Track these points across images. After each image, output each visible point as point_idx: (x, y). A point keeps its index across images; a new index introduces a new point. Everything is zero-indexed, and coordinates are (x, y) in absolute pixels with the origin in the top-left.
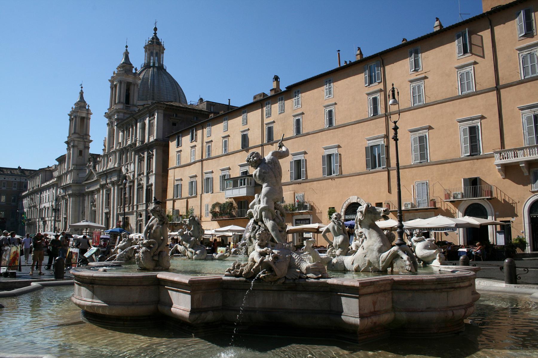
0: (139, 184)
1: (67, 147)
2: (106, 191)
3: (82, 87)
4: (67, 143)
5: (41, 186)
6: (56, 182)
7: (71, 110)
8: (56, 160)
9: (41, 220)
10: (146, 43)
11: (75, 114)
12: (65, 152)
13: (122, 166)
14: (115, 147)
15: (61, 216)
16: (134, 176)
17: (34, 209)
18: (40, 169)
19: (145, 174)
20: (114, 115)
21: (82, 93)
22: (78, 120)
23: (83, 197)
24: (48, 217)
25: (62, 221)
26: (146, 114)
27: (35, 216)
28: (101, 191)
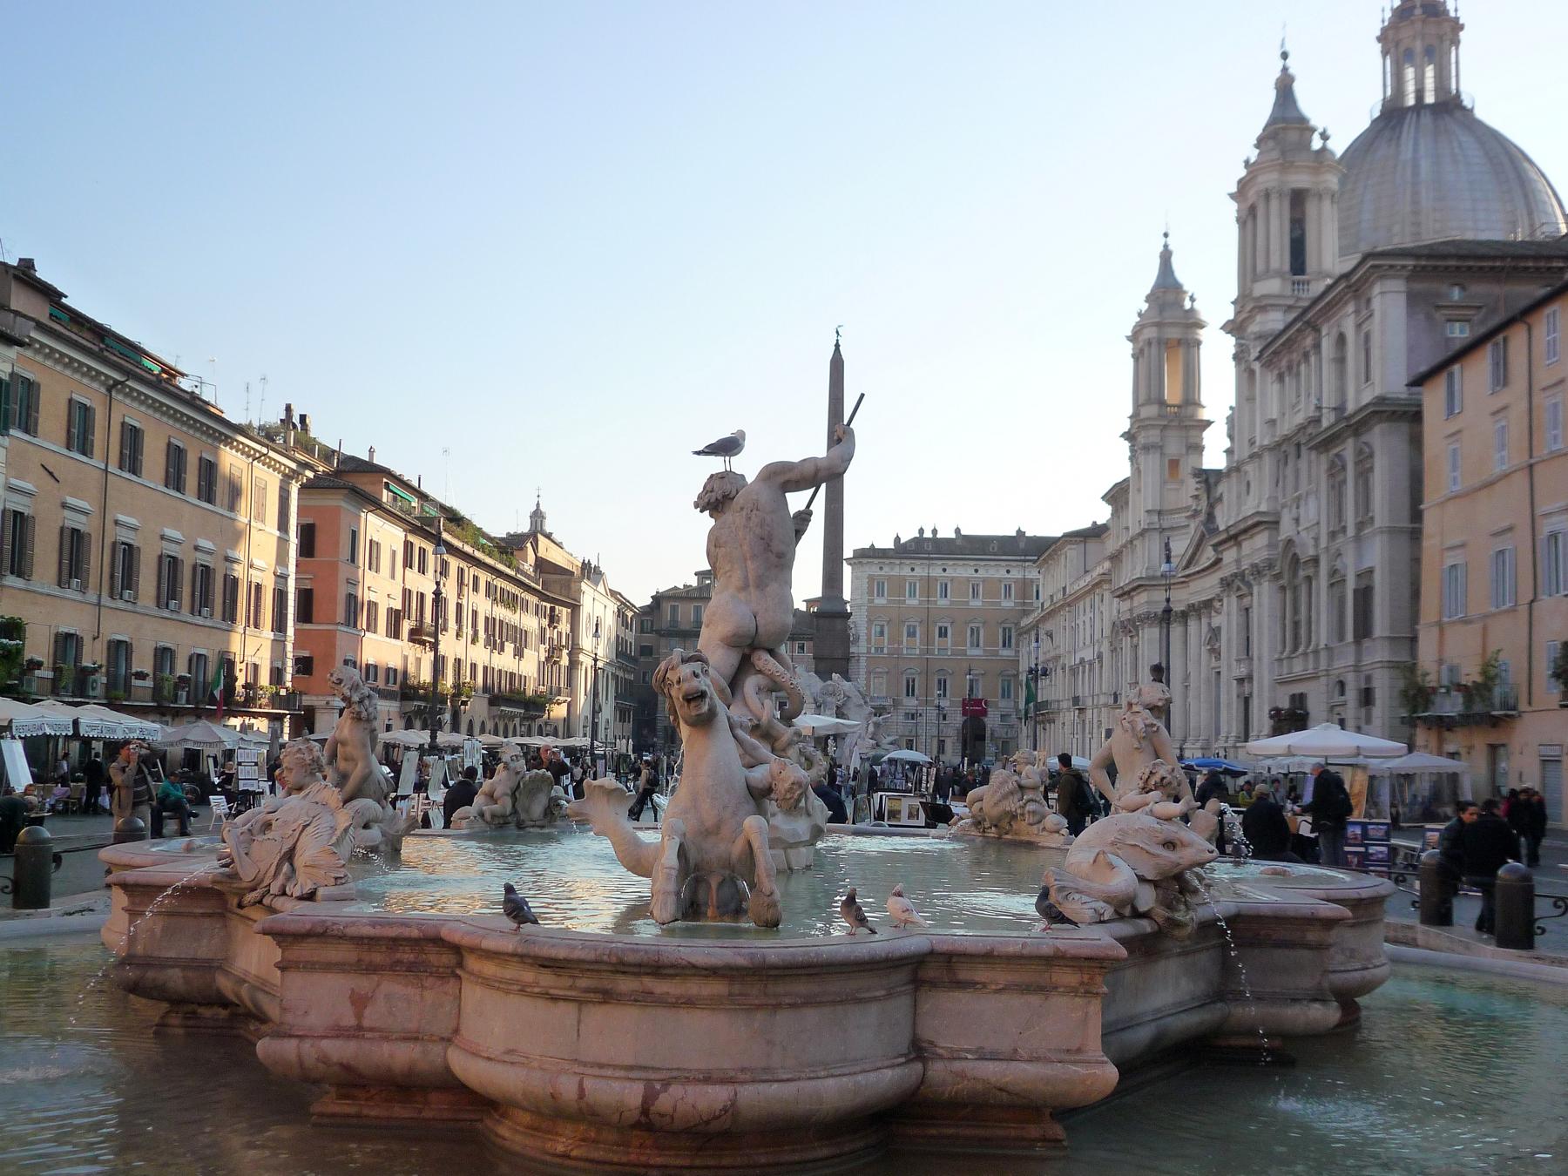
0: (1333, 572)
3: (1166, 235)
4: (1128, 436)
6: (1104, 577)
8: (1103, 498)
10: (1383, 21)
12: (1123, 471)
13: (1284, 506)
14: (1264, 439)
16: (1316, 539)
18: (1066, 535)
19: (1351, 532)
21: (1166, 256)
23: (1186, 625)
26: (1346, 303)
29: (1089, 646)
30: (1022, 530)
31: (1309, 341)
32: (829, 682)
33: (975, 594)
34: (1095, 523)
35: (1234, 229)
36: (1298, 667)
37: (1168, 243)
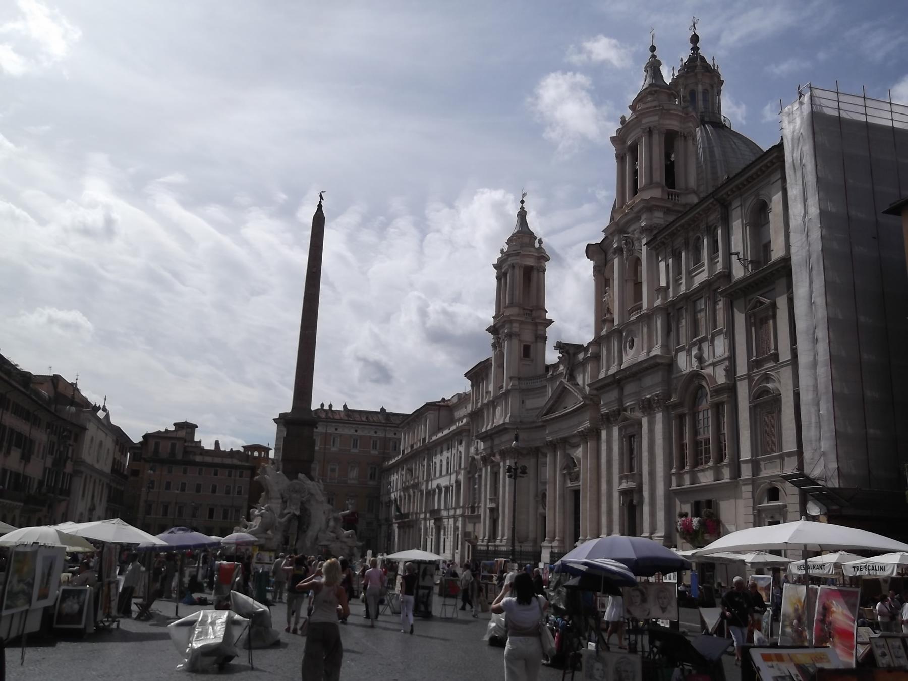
1: (493, 341)
2: (620, 429)
3: (522, 202)
5: (429, 441)
6: (466, 427)
7: (500, 255)
8: (466, 375)
9: (430, 515)
10: (674, 75)
11: (511, 261)
12: (488, 353)
13: (677, 351)
15: (482, 505)
16: (731, 371)
17: (414, 493)
20: (638, 218)
22: (519, 274)
24: (446, 509)
25: (485, 519)
27: (415, 507)
28: (604, 434)
29: (445, 476)
30: (384, 408)
31: (714, 217)
32: (295, 481)
33: (355, 446)
34: (443, 399)
35: (613, 163)
36: (706, 478)
37: (524, 206)
